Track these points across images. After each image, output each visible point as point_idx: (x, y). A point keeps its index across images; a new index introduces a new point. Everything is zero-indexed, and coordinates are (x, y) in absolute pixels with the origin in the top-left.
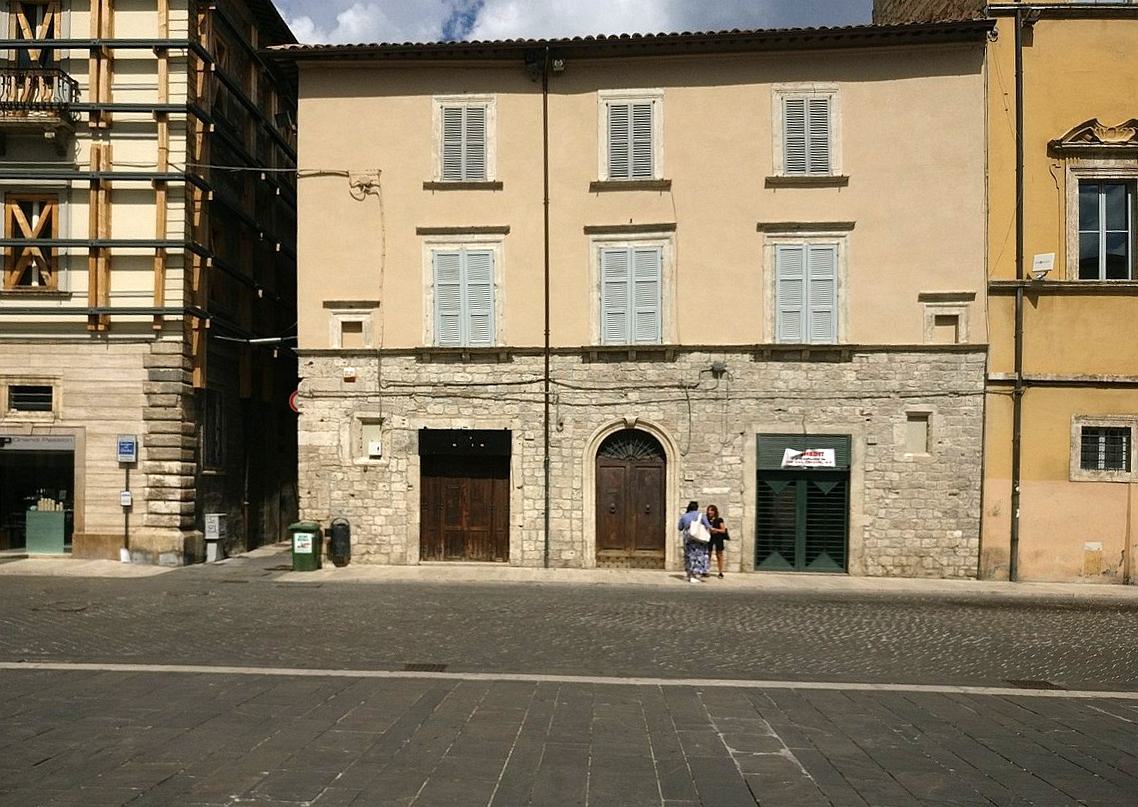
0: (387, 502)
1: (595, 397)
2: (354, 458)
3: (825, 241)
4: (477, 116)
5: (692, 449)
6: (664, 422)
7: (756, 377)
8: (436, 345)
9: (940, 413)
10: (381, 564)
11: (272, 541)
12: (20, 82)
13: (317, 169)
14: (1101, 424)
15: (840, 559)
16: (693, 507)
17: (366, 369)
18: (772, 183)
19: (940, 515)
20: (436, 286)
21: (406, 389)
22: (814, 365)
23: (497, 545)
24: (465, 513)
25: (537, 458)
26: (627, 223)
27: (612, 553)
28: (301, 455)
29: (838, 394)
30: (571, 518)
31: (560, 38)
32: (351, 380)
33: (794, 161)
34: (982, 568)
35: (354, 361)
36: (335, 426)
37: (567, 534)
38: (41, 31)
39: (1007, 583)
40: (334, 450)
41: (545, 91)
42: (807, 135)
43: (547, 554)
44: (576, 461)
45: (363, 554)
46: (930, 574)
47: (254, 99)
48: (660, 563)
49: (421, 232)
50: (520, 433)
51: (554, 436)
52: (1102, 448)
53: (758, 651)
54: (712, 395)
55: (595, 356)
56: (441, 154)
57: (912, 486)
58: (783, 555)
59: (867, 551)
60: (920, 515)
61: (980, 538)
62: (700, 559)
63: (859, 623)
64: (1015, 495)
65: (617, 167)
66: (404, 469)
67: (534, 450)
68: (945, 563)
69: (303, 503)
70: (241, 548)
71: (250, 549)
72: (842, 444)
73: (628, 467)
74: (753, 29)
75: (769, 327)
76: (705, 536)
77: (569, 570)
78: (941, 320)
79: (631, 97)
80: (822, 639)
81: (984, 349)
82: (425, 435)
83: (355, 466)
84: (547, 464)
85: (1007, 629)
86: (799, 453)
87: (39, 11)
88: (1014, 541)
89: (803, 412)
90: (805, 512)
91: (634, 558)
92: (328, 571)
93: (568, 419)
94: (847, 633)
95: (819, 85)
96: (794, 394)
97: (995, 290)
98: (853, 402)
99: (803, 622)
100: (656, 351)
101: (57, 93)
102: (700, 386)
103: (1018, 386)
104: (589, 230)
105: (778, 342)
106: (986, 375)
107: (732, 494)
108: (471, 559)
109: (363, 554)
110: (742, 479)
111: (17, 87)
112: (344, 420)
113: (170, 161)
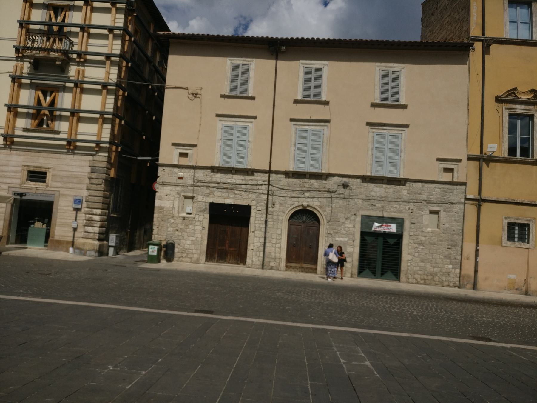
0: (193, 234)
1: (290, 193)
2: (179, 214)
3: (396, 132)
4: (246, 68)
5: (332, 220)
6: (320, 207)
7: (362, 190)
8: (221, 165)
9: (444, 211)
10: (187, 262)
11: (139, 248)
12: (48, 40)
13: (174, 85)
14: (517, 221)
15: (396, 274)
16: (331, 246)
17: (188, 174)
18: (374, 105)
19: (443, 257)
20: (222, 140)
21: (206, 184)
22: (389, 186)
23: (241, 257)
24: (227, 242)
25: (262, 219)
26: (309, 118)
27: (293, 265)
28: (156, 210)
29: (399, 200)
30: (275, 247)
31: (285, 37)
32: (181, 178)
33: (384, 96)
34: (461, 283)
35: (183, 170)
36: (172, 198)
37: (273, 254)
38: (60, 19)
39: (472, 291)
40: (171, 209)
41: (277, 59)
42: (390, 85)
43: (263, 263)
44: (280, 221)
45: (180, 257)
46: (437, 284)
47: (149, 54)
48: (314, 271)
49: (218, 116)
50: (255, 207)
51: (270, 209)
52: (517, 232)
53: (357, 314)
54: (342, 196)
55: (291, 175)
56: (229, 83)
57: (430, 244)
58: (371, 271)
59: (409, 271)
60: (434, 257)
61: (460, 269)
62: (333, 270)
63: (404, 305)
64: (477, 251)
65: (306, 93)
66: (201, 220)
67: (260, 215)
68: (444, 279)
69: (155, 232)
70: (125, 250)
71: (129, 251)
72: (400, 222)
73: (303, 226)
74: (369, 39)
75: (369, 168)
76: (335, 259)
77: (273, 271)
78: (446, 170)
79: (314, 64)
80: (386, 311)
81: (465, 184)
82: (212, 205)
83: (180, 217)
84: (266, 222)
85: (470, 312)
86: (380, 225)
87: (60, 10)
88: (476, 271)
89: (383, 207)
90: (382, 252)
91: (303, 268)
92: (163, 264)
93: (277, 202)
94: (398, 309)
95: (396, 65)
96: (379, 198)
97: (471, 158)
98: (405, 204)
99: (378, 302)
100: (318, 175)
101: (63, 45)
102: (337, 192)
103: (479, 202)
104: (292, 120)
105: (373, 175)
106: (465, 196)
107: (349, 241)
108: (229, 263)
109: (180, 257)
110: (354, 235)
111: (47, 42)
112: (176, 196)
113: (110, 77)
